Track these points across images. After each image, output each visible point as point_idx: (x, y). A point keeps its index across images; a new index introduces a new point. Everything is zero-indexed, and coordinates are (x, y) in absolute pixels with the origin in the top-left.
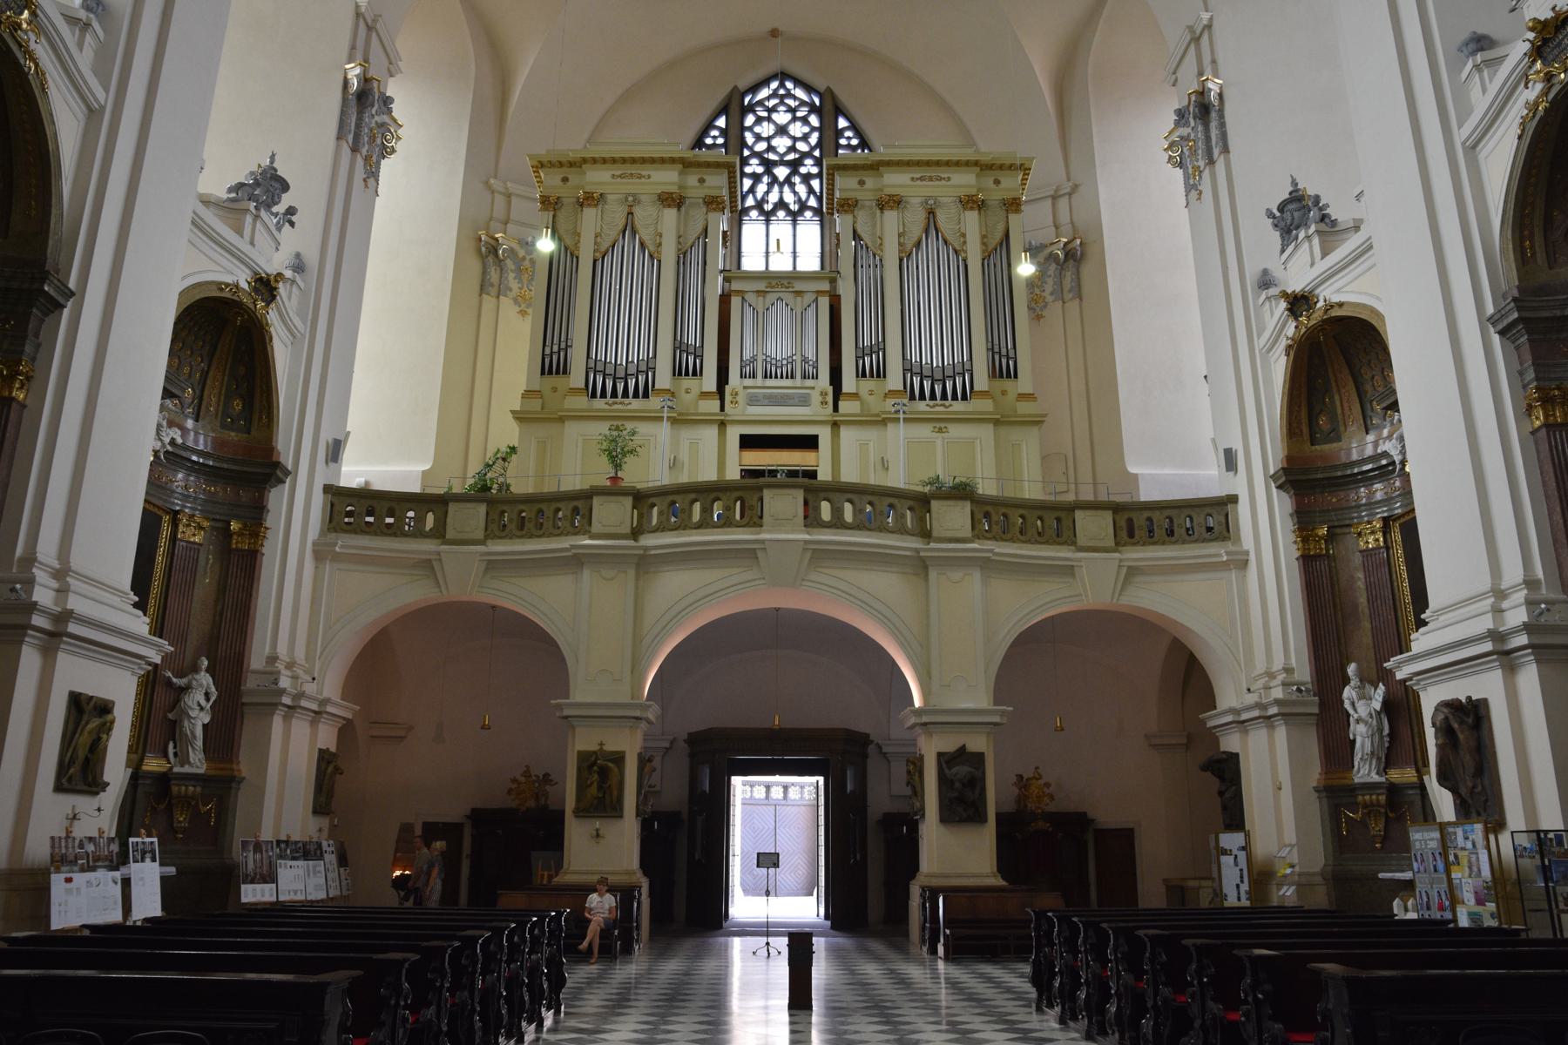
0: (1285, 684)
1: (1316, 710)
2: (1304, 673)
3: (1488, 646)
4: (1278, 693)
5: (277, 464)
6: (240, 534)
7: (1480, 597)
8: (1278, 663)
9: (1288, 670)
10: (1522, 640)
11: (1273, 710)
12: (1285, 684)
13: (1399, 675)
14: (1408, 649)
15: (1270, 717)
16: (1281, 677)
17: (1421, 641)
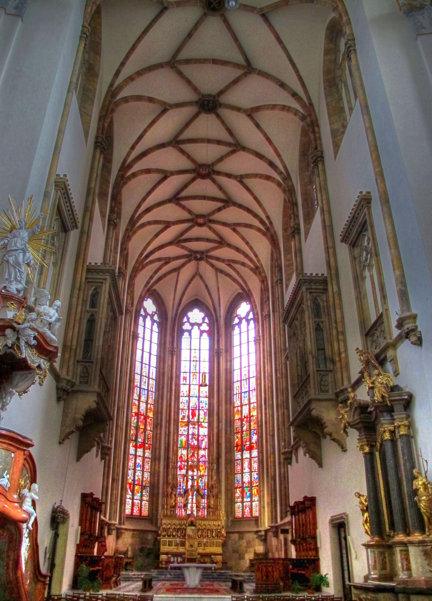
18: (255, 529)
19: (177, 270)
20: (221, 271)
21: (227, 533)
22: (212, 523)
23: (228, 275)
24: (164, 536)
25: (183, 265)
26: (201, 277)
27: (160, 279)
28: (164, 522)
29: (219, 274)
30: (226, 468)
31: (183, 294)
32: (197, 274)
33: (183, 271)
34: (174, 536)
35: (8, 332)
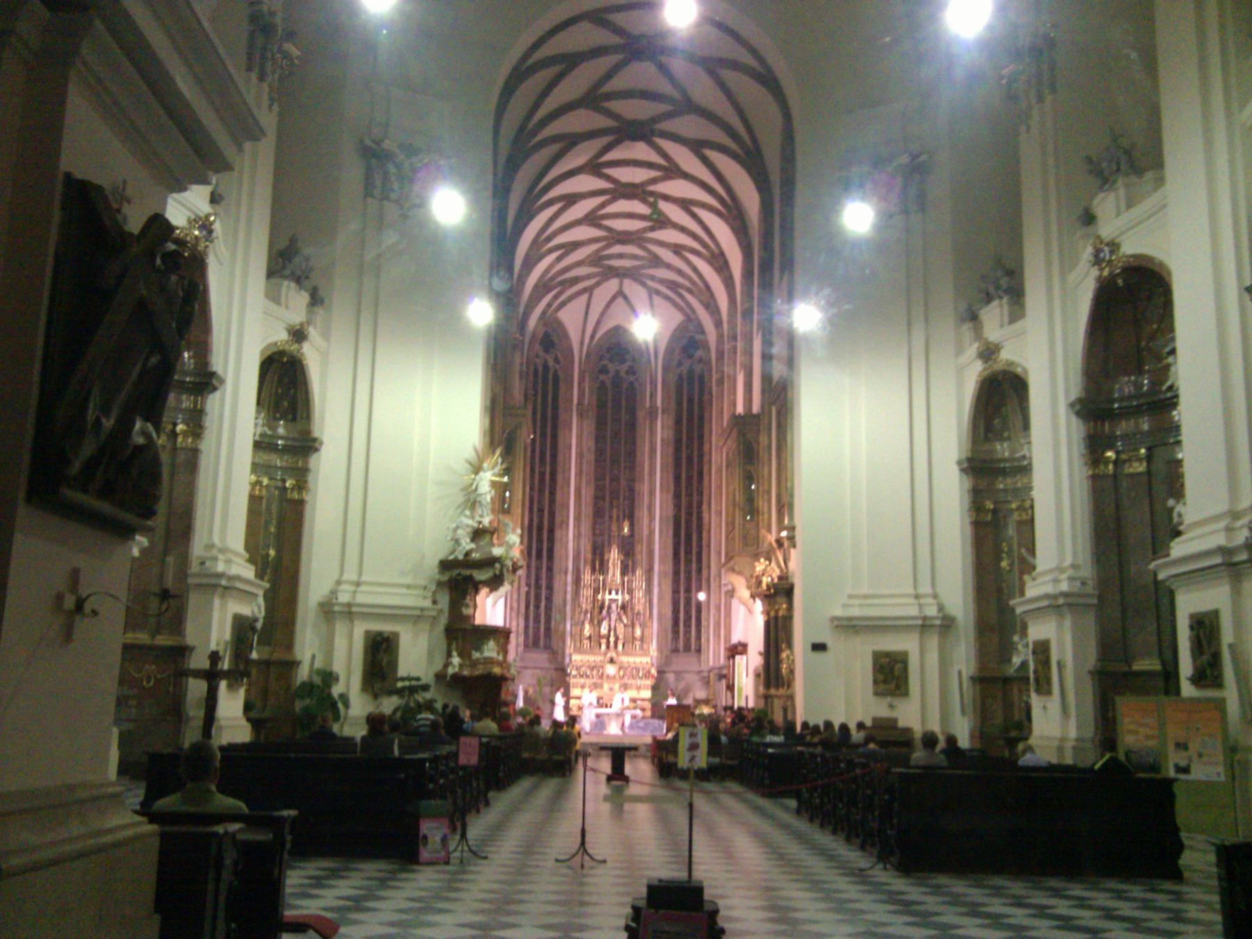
0: (1071, 579)
1: (1095, 601)
2: (1088, 572)
3: (1218, 560)
4: (1064, 587)
5: (213, 374)
6: (184, 433)
7: (1217, 518)
8: (1069, 560)
9: (1073, 566)
10: (1244, 556)
11: (1061, 601)
12: (1071, 579)
13: (1161, 576)
14: (1168, 555)
15: (1059, 606)
16: (1070, 572)
17: (1178, 549)
18: (696, 668)
19: (589, 290)
20: (658, 292)
21: (659, 672)
22: (638, 660)
23: (667, 298)
24: (575, 677)
25: (598, 284)
26: (626, 298)
27: (563, 304)
28: (574, 658)
29: (655, 297)
30: (660, 585)
31: (598, 323)
32: (620, 293)
33: (596, 292)
34: (587, 677)
35: (497, 565)
